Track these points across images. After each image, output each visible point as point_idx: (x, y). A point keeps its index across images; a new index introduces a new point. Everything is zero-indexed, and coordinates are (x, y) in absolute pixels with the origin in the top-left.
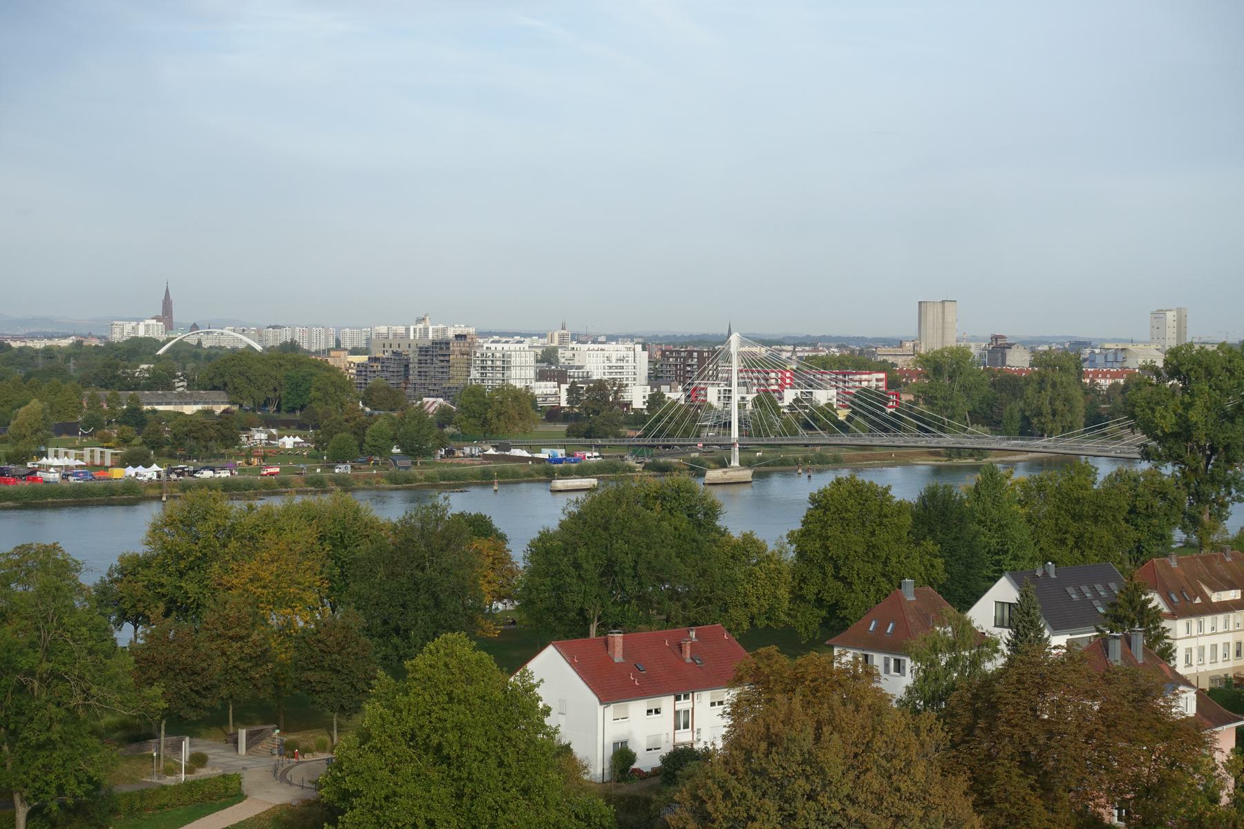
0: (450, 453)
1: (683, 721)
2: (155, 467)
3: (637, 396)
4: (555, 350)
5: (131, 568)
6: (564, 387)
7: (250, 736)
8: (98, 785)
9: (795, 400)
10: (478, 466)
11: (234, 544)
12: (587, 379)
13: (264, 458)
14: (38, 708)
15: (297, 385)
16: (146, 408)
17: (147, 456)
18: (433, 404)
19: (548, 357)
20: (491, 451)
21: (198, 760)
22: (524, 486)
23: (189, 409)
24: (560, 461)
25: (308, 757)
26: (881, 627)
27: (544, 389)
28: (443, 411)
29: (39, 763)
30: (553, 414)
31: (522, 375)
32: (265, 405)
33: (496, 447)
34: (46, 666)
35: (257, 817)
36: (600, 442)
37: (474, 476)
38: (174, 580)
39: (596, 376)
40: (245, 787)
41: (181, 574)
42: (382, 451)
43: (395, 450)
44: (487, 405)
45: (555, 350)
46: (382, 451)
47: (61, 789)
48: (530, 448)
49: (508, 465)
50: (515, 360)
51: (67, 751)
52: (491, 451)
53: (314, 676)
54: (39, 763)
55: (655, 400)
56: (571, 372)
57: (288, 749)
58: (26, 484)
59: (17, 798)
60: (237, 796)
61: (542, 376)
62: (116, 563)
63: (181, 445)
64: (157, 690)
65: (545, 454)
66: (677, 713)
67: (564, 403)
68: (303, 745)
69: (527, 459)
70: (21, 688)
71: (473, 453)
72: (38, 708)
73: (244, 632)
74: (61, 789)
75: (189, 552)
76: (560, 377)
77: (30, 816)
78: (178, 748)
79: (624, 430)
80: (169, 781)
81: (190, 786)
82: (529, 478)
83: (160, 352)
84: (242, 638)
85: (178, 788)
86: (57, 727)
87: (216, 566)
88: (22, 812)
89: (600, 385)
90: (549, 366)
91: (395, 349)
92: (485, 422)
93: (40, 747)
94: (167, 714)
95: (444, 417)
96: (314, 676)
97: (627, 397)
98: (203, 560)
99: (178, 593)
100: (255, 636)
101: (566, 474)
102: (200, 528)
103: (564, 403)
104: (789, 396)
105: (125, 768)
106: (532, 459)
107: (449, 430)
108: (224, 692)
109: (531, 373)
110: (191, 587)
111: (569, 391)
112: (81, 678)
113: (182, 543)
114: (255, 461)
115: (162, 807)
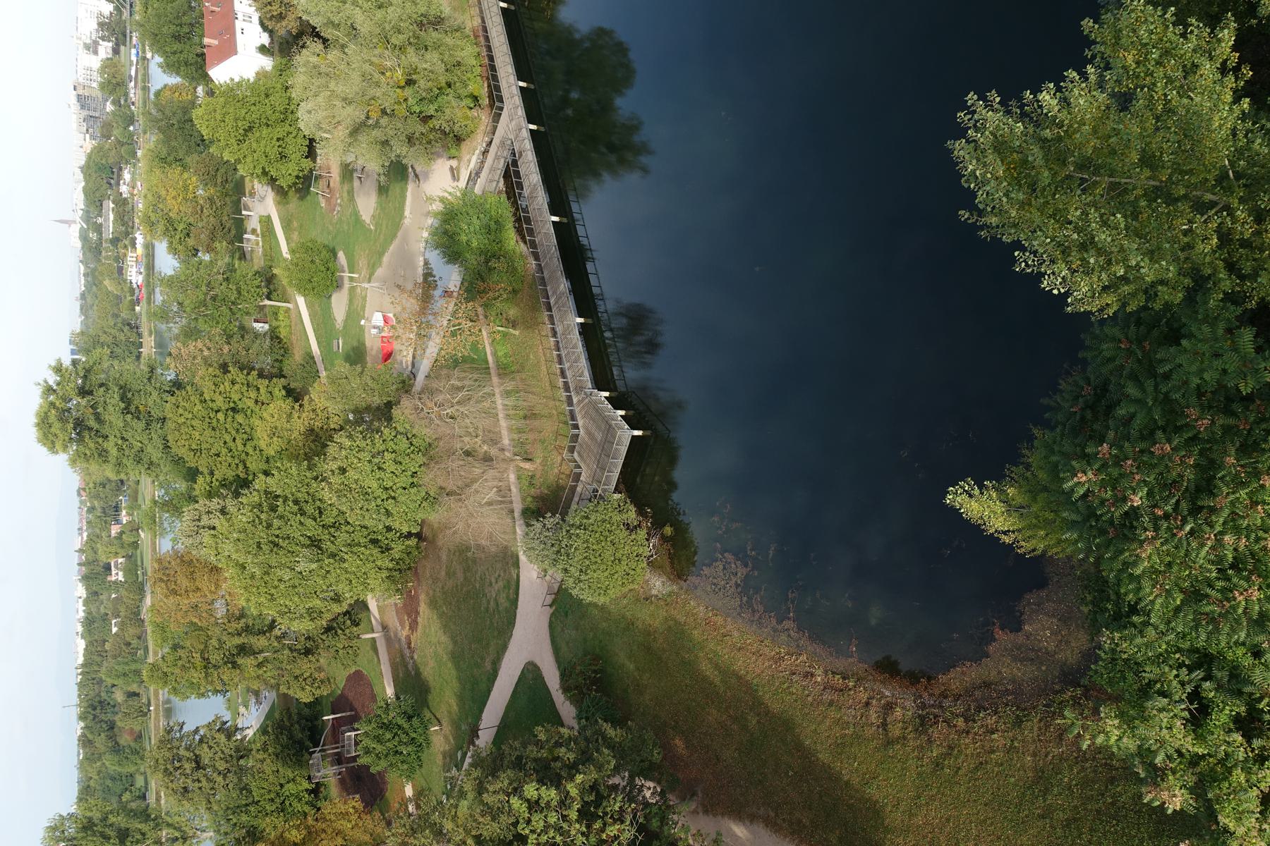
0: (133, 103)
2: (137, 235)
4: (85, 44)
5: (173, 250)
7: (245, 210)
8: (257, 273)
10: (139, 92)
11: (161, 206)
12: (97, 31)
13: (133, 188)
14: (222, 293)
15: (100, 168)
16: (111, 236)
17: (132, 238)
18: (109, 107)
19: (87, 47)
20: (132, 84)
21: (254, 231)
22: (150, 72)
24: (138, 52)
25: (255, 187)
28: (113, 103)
29: (246, 294)
30: (116, 51)
31: (95, 62)
32: (110, 184)
33: (131, 81)
34: (204, 288)
35: (277, 211)
36: (128, 31)
37: (144, 94)
38: (178, 233)
39: (96, 27)
40: (266, 214)
41: (176, 229)
42: (131, 135)
43: (131, 128)
44: (109, 82)
45: (85, 44)
46: (131, 135)
47: (258, 287)
48: (131, 65)
49: (140, 77)
50: (88, 65)
51: (241, 283)
52: (132, 84)
53: (219, 180)
54: (246, 294)
56: (94, 38)
57: (252, 195)
58: (143, 289)
59: (261, 304)
60: (269, 217)
62: (171, 256)
63: (127, 223)
64: (217, 245)
65: (134, 58)
68: (250, 188)
69: (137, 69)
70: (214, 298)
71: (134, 93)
72: (222, 293)
73: (199, 207)
74: (258, 287)
75: (165, 225)
77: (269, 299)
78: (248, 240)
79: (124, 18)
80: (261, 244)
81: (263, 236)
82: (146, 68)
84: (202, 208)
85: (263, 242)
86: (230, 286)
87: (171, 214)
88: (267, 302)
89: (101, 25)
90: (92, 48)
91: (82, 120)
92: (118, 84)
93: (239, 293)
94: (231, 243)
95: (116, 103)
96: (219, 180)
97: (107, 13)
98: (170, 221)
99: (184, 231)
100: (201, 202)
101: (144, 52)
102: (153, 219)
103: (110, 44)
105: (255, 261)
106: (137, 65)
107: (122, 102)
108: (226, 218)
109: (93, 57)
110: (181, 227)
111: (103, 40)
112: (209, 275)
113: (160, 228)
114: (135, 192)
115: (271, 249)
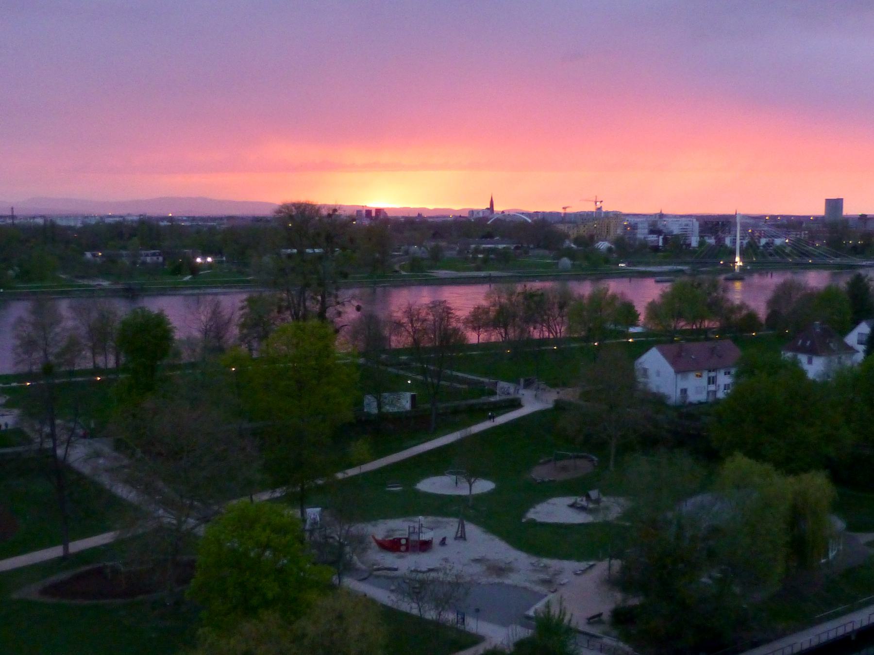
1: (712, 381)
3: (694, 242)
6: (661, 237)
9: (767, 243)
23: (500, 246)
26: (804, 342)
27: (652, 238)
30: (656, 249)
50: (640, 226)
55: (702, 243)
61: (652, 232)
66: (709, 378)
67: (661, 244)
76: (658, 232)
83: (489, 223)
104: (763, 241)
109: (646, 231)
